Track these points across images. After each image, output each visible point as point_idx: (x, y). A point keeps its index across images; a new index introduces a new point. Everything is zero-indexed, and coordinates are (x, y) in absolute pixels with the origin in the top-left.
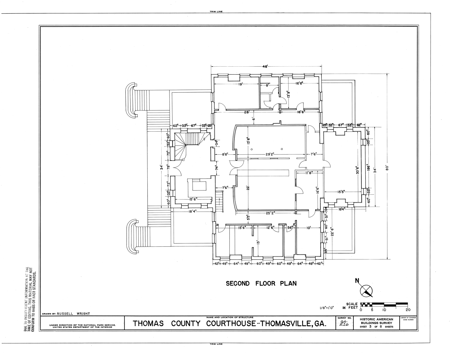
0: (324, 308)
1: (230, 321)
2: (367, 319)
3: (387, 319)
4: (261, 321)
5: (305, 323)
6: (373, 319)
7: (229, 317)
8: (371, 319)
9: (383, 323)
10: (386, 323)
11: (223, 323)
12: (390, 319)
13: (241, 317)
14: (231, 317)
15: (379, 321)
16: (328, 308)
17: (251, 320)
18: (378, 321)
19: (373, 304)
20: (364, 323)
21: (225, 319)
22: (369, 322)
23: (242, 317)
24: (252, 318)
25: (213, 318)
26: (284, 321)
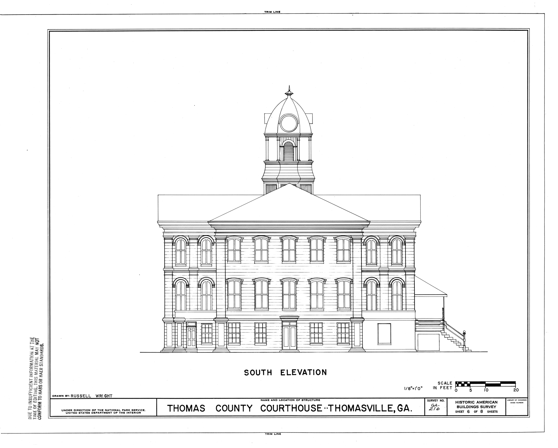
0: (409, 389)
1: (290, 405)
2: (464, 402)
3: (490, 402)
4: (329, 405)
5: (385, 408)
6: (472, 402)
7: (289, 400)
8: (469, 402)
9: (484, 407)
10: (488, 407)
11: (281, 408)
12: (493, 401)
13: (305, 400)
14: (292, 399)
15: (479, 405)
16: (415, 389)
17: (316, 403)
18: (478, 405)
19: (472, 383)
20: (461, 407)
21: (284, 403)
22: (467, 406)
23: (306, 400)
24: (319, 400)
25: (268, 400)
26: (358, 405)
